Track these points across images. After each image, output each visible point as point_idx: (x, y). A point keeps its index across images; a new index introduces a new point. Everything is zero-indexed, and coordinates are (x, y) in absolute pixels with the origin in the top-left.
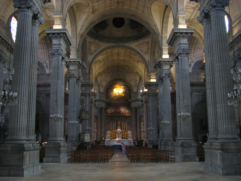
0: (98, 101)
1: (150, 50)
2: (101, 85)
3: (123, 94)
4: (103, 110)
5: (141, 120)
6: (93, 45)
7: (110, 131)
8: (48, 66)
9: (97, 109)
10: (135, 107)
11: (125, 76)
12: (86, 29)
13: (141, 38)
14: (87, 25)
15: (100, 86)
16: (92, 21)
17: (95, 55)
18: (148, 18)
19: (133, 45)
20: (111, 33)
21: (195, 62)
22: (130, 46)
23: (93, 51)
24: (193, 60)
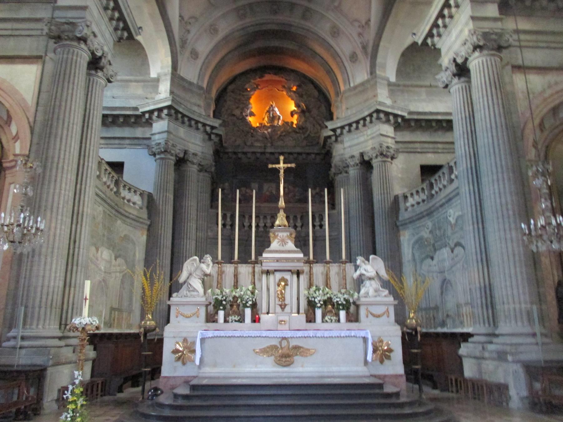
0: (165, 111)
2: (184, 43)
3: (296, 116)
4: (192, 170)
5: (401, 218)
7: (208, 258)
9: (158, 157)
10: (362, 155)
11: (307, 10)
15: (183, 46)
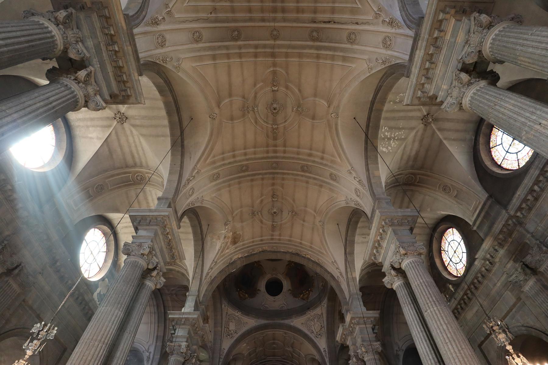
1: (325, 330)
8: (151, 357)
12: (220, 272)
13: (309, 309)
14: (224, 263)
16: (231, 259)
17: (235, 338)
18: (319, 251)
19: (297, 322)
21: (404, 349)
22: (292, 324)
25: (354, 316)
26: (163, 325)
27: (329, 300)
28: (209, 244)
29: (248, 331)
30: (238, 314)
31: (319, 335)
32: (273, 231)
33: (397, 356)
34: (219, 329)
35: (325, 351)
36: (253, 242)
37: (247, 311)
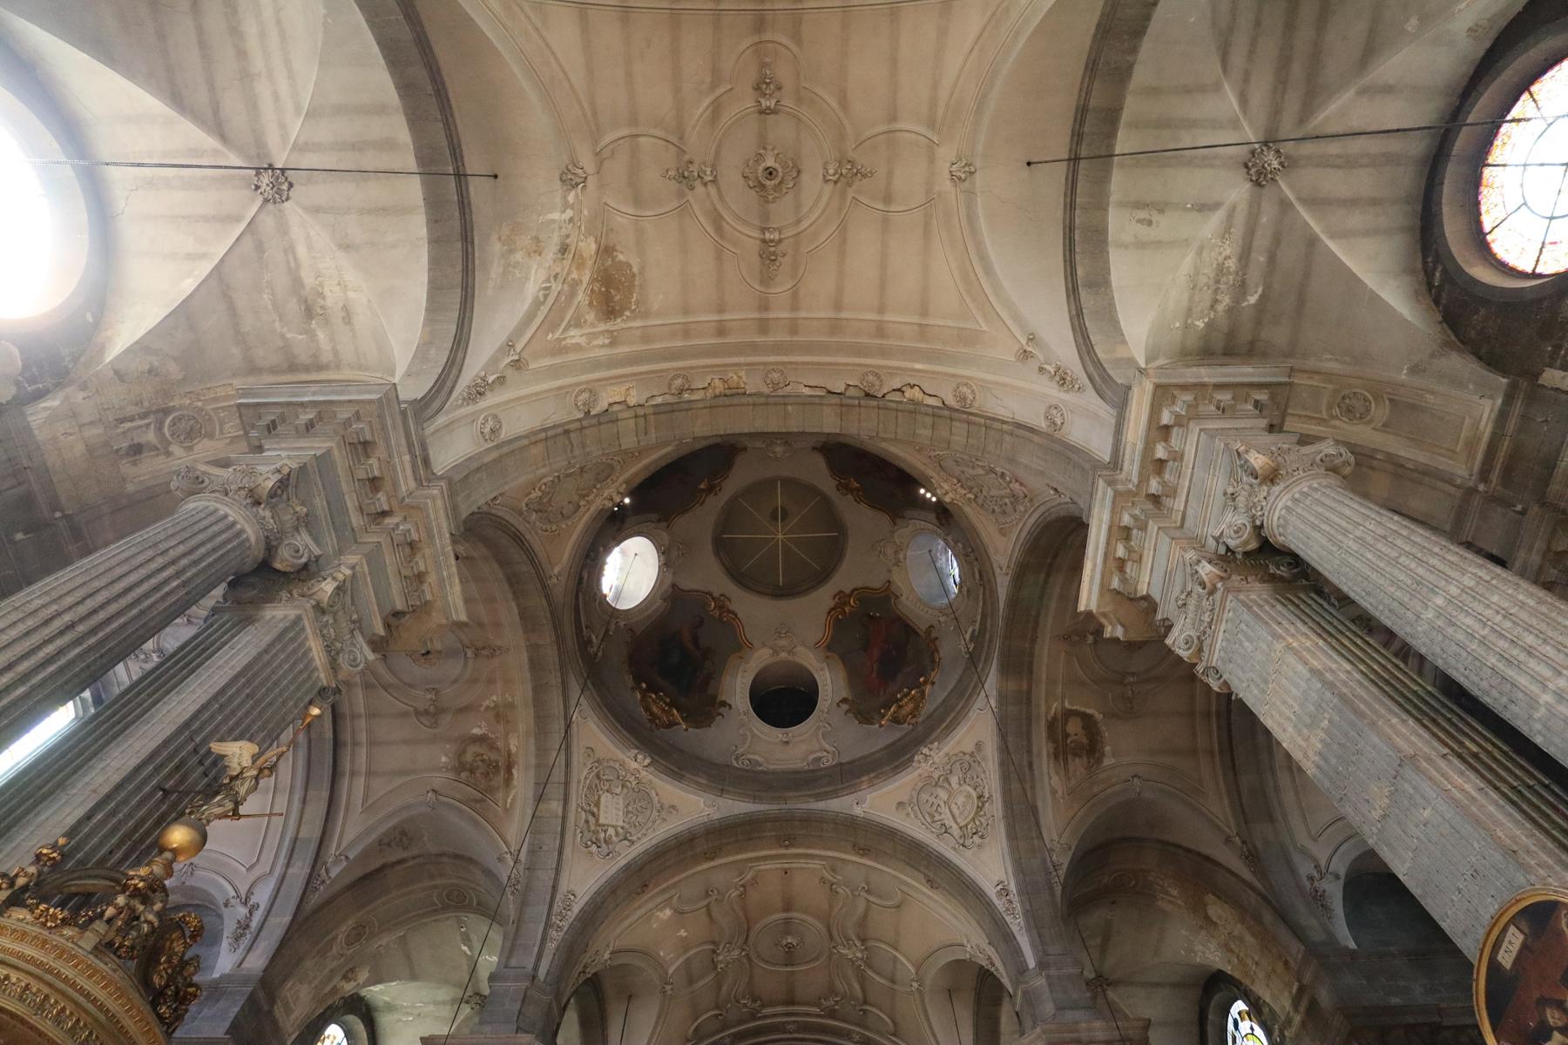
1: (996, 808)
6: (618, 790)
19: (879, 802)
20: (740, 751)
21: (1342, 872)
22: (858, 811)
23: (611, 831)
24: (1323, 863)
25: (1164, 381)
26: (325, 794)
27: (1006, 670)
28: (495, 270)
29: (676, 837)
30: (635, 763)
31: (972, 834)
32: (766, 280)
33: (1318, 899)
34: (556, 806)
35: (1004, 892)
36: (686, 331)
37: (680, 763)
